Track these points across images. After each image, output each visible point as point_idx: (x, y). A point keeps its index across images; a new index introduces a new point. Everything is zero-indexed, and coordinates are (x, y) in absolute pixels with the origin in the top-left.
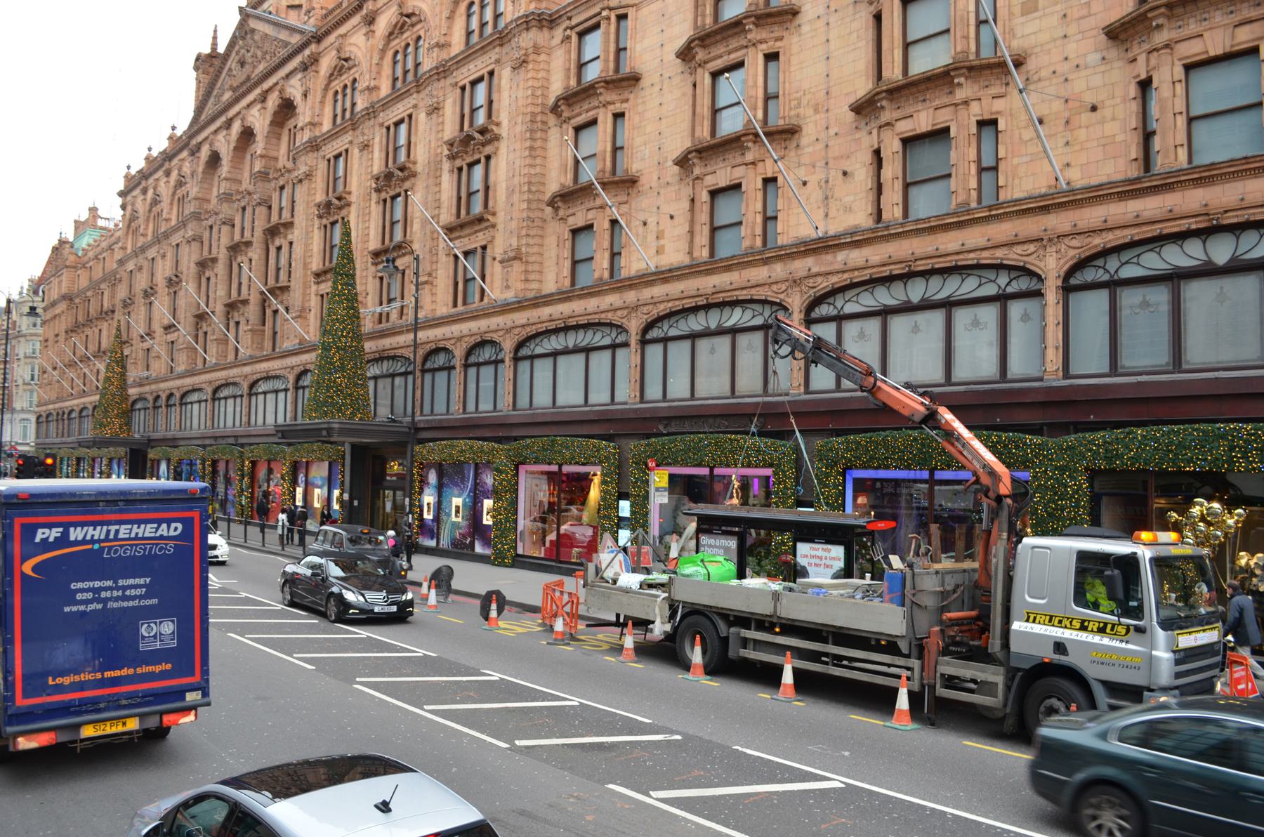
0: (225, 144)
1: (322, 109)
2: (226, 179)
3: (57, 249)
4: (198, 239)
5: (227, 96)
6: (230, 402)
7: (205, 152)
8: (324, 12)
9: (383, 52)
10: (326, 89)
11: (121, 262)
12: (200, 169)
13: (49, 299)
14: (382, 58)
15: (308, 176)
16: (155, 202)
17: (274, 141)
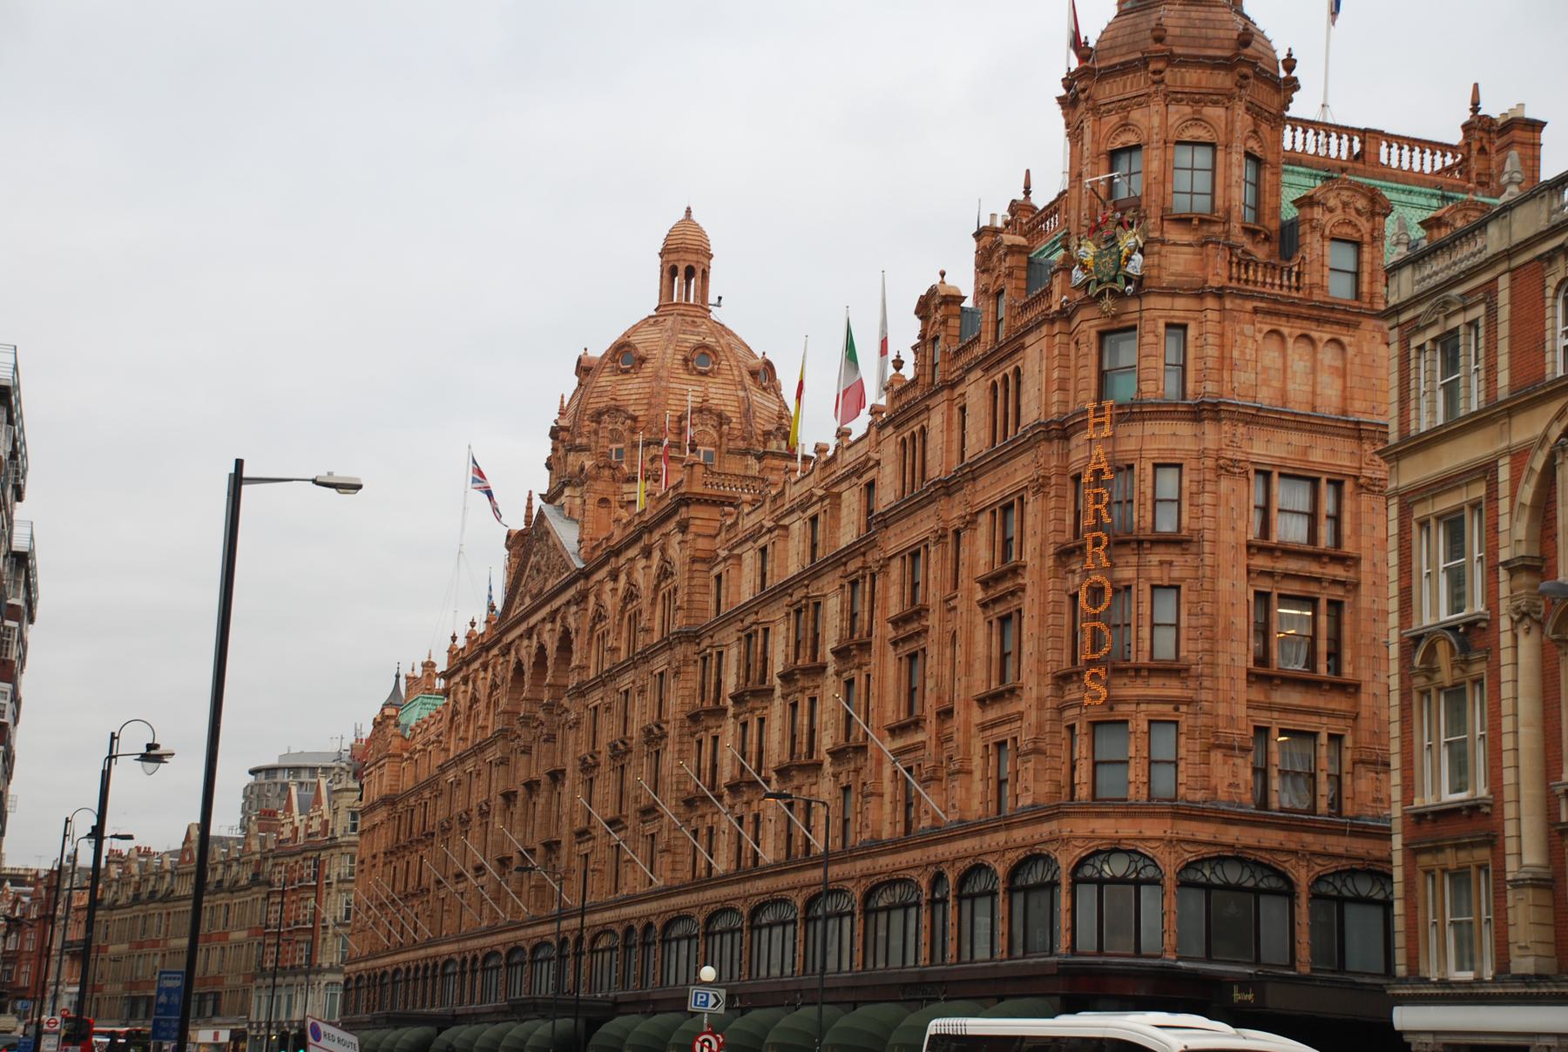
0: (527, 650)
1: (589, 652)
2: (525, 699)
3: (380, 723)
4: (504, 762)
5: (528, 601)
6: (777, 931)
7: (512, 657)
8: (595, 543)
9: (622, 612)
10: (592, 629)
11: (443, 769)
12: (510, 675)
13: (368, 797)
14: (622, 619)
15: (577, 723)
16: (474, 700)
17: (563, 667)
